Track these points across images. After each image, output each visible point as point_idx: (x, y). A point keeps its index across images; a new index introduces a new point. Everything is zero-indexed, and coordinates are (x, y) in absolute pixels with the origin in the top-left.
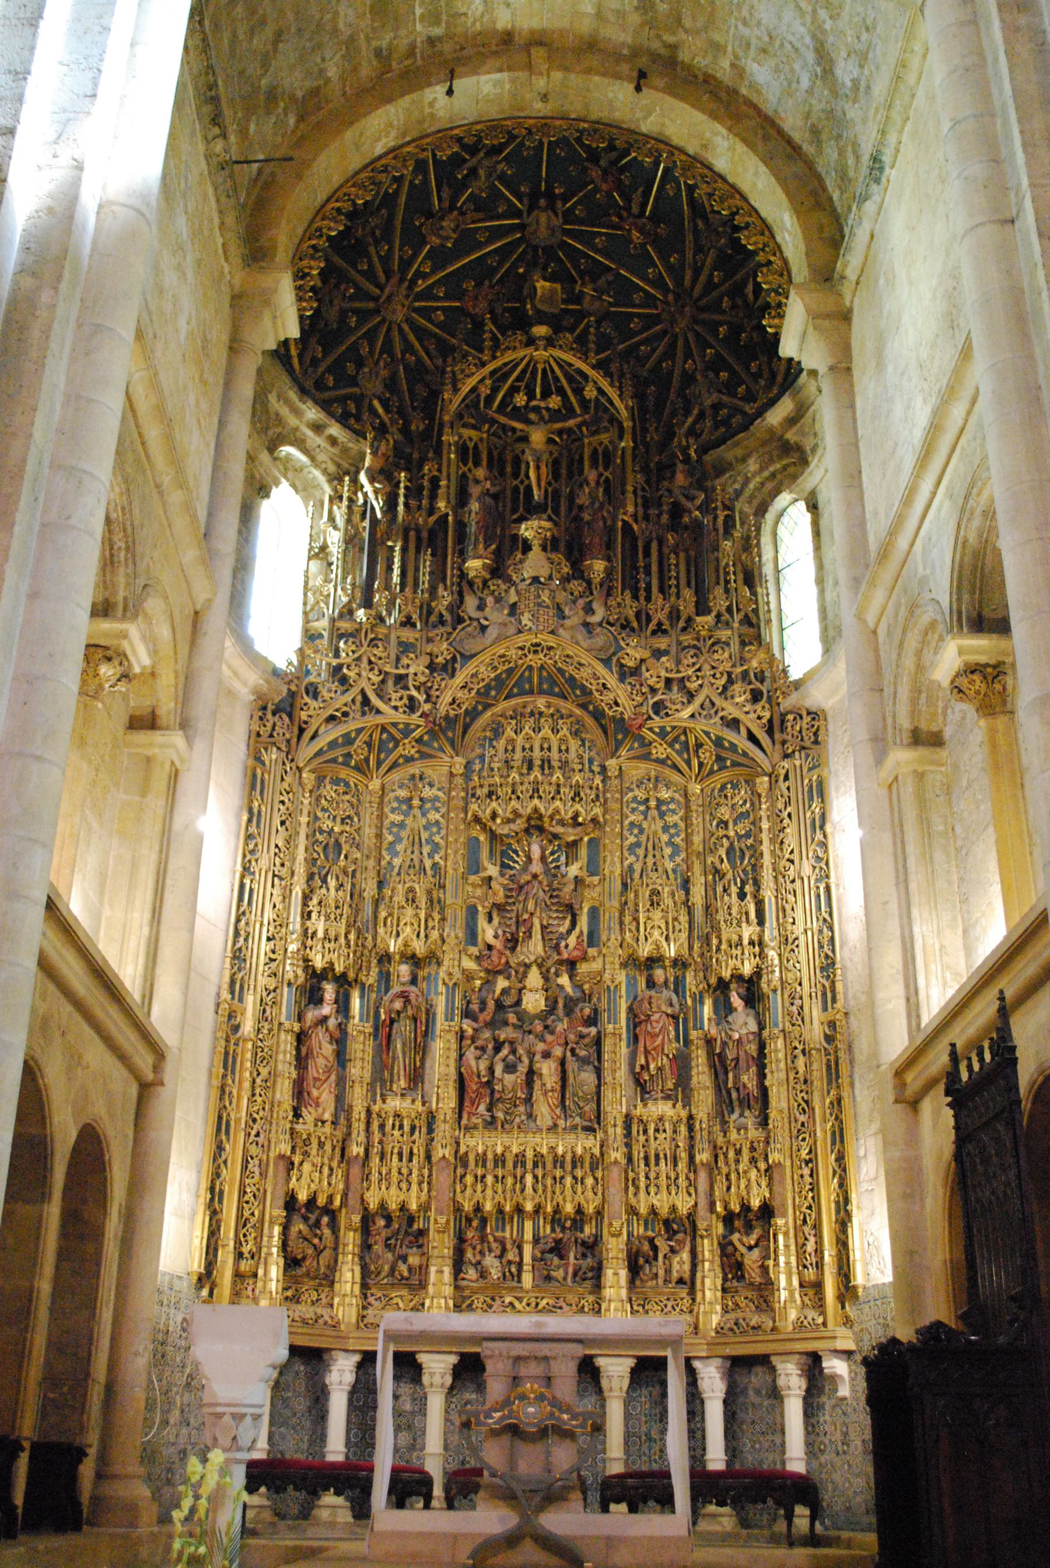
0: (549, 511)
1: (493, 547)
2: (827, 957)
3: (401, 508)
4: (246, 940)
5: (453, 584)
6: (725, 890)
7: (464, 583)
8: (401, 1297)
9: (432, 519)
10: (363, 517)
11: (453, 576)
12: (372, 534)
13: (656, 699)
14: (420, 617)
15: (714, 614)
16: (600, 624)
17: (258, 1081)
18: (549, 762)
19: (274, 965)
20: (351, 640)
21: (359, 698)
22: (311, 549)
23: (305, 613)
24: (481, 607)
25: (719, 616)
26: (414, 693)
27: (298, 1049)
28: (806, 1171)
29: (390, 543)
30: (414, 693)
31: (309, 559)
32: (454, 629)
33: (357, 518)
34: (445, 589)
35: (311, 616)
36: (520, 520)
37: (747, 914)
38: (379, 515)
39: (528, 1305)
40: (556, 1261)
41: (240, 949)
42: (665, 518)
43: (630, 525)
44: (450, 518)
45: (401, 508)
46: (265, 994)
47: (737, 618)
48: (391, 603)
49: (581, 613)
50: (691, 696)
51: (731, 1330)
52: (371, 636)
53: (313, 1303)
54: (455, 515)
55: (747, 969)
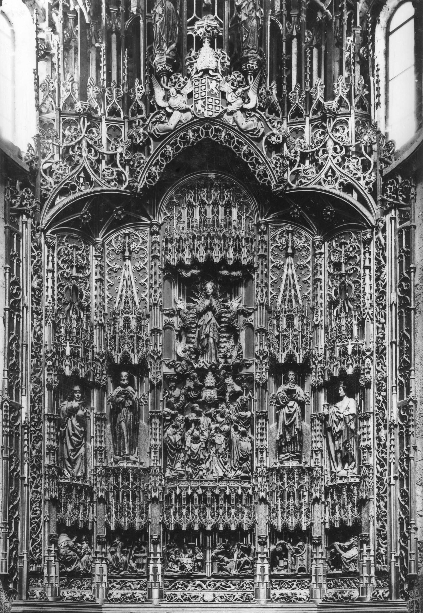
0: (216, 15)
1: (174, 45)
2: (405, 361)
3: (104, 13)
4: (17, 357)
5: (145, 78)
6: (338, 315)
7: (154, 81)
8: (132, 582)
9: (128, 23)
10: (75, 24)
11: (145, 71)
12: (83, 35)
13: (294, 170)
14: (123, 108)
15: (337, 99)
16: (254, 110)
17: (34, 452)
18: (218, 221)
19: (37, 375)
20: (73, 127)
21: (82, 175)
22: (37, 53)
23: (38, 107)
24: (166, 98)
25: (341, 100)
26: (121, 169)
27: (58, 430)
28: (382, 503)
29: (97, 45)
30: (121, 169)
31: (38, 60)
32: (148, 117)
33: (71, 24)
34: (140, 83)
35: (44, 110)
36: (192, 23)
37: (352, 332)
38: (87, 19)
39: (210, 585)
40: (226, 559)
41: (14, 364)
42: (303, 17)
43: (277, 24)
44: (141, 22)
45: (104, 13)
46: (33, 395)
47: (355, 101)
48: (100, 98)
49: (240, 101)
50: (320, 167)
51: (331, 599)
52: (87, 124)
53: (79, 588)
54: (145, 17)
55: (350, 371)
